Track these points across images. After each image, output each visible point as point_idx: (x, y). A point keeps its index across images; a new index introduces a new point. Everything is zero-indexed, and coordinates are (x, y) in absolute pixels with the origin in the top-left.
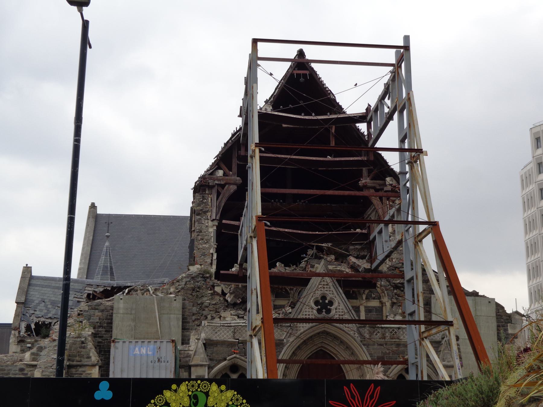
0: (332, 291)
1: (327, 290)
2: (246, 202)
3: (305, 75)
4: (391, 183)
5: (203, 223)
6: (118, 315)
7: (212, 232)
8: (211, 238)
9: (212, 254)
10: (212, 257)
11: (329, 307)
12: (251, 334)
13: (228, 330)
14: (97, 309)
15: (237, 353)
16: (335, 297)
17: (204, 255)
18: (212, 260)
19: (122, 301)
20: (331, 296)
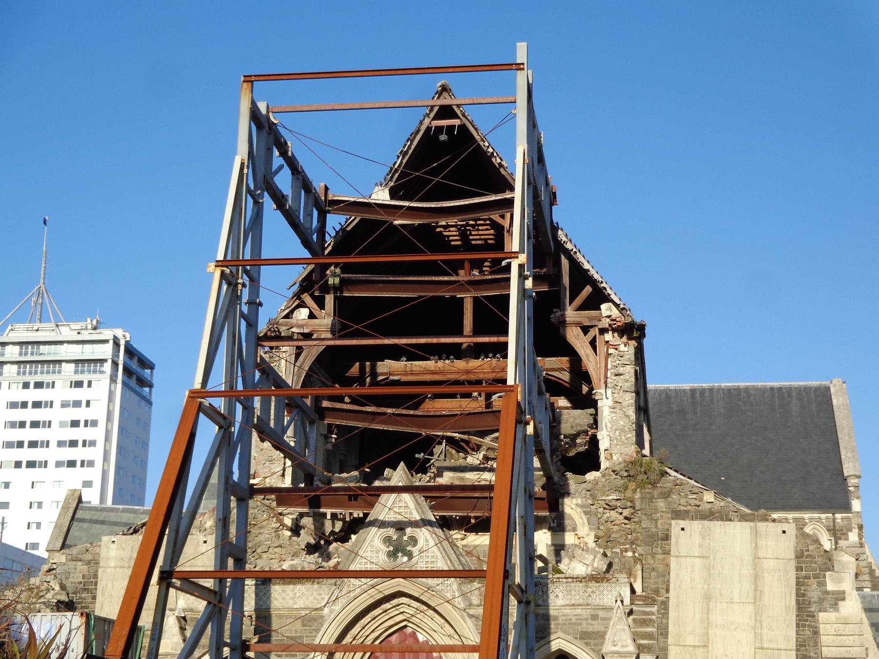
3: (451, 128)
4: (608, 313)
6: (106, 570)
11: (409, 548)
14: (81, 561)
19: (114, 546)
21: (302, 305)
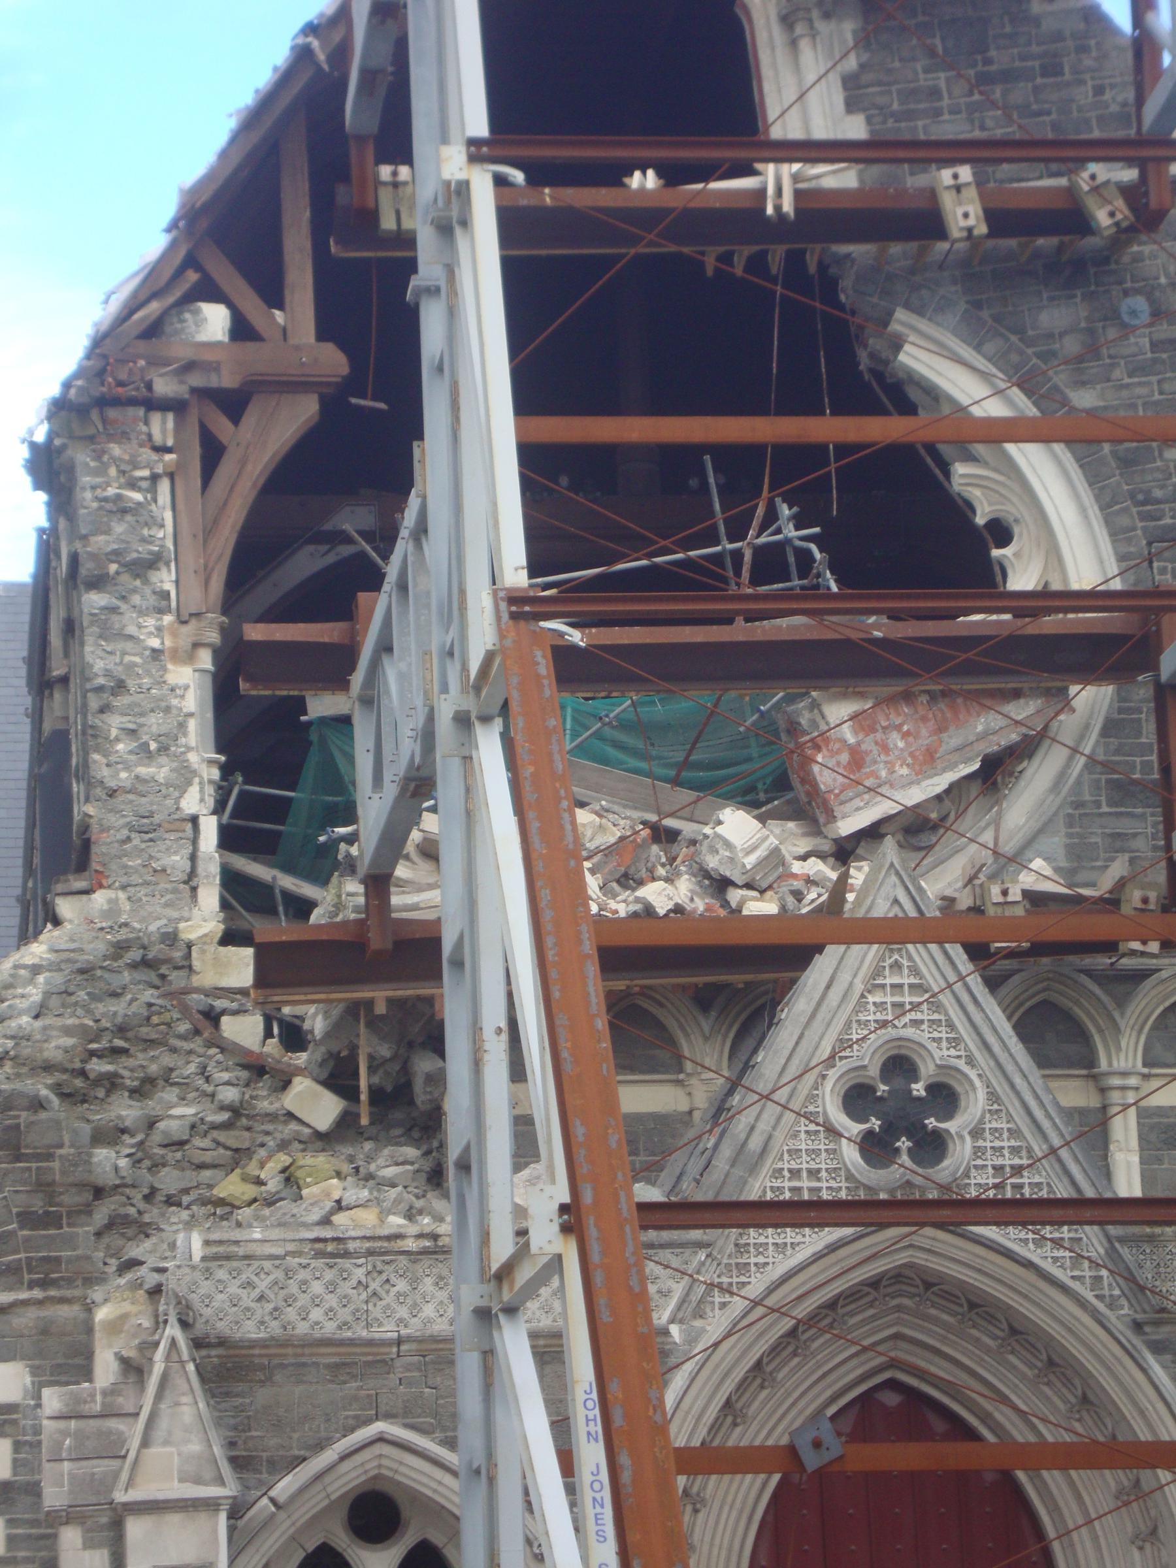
0: (951, 1026)
1: (916, 1023)
2: (414, 502)
5: (131, 637)
7: (186, 687)
8: (182, 726)
9: (194, 820)
10: (195, 841)
11: (931, 1122)
12: (483, 1303)
13: (329, 1275)
15: (388, 1416)
16: (971, 1061)
17: (147, 829)
18: (193, 858)
20: (942, 1053)
21: (210, 292)
